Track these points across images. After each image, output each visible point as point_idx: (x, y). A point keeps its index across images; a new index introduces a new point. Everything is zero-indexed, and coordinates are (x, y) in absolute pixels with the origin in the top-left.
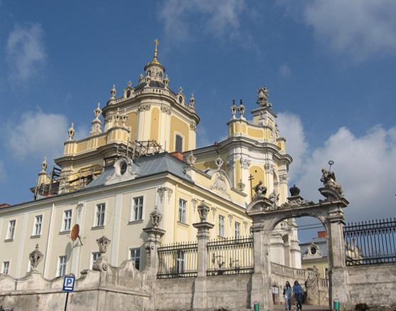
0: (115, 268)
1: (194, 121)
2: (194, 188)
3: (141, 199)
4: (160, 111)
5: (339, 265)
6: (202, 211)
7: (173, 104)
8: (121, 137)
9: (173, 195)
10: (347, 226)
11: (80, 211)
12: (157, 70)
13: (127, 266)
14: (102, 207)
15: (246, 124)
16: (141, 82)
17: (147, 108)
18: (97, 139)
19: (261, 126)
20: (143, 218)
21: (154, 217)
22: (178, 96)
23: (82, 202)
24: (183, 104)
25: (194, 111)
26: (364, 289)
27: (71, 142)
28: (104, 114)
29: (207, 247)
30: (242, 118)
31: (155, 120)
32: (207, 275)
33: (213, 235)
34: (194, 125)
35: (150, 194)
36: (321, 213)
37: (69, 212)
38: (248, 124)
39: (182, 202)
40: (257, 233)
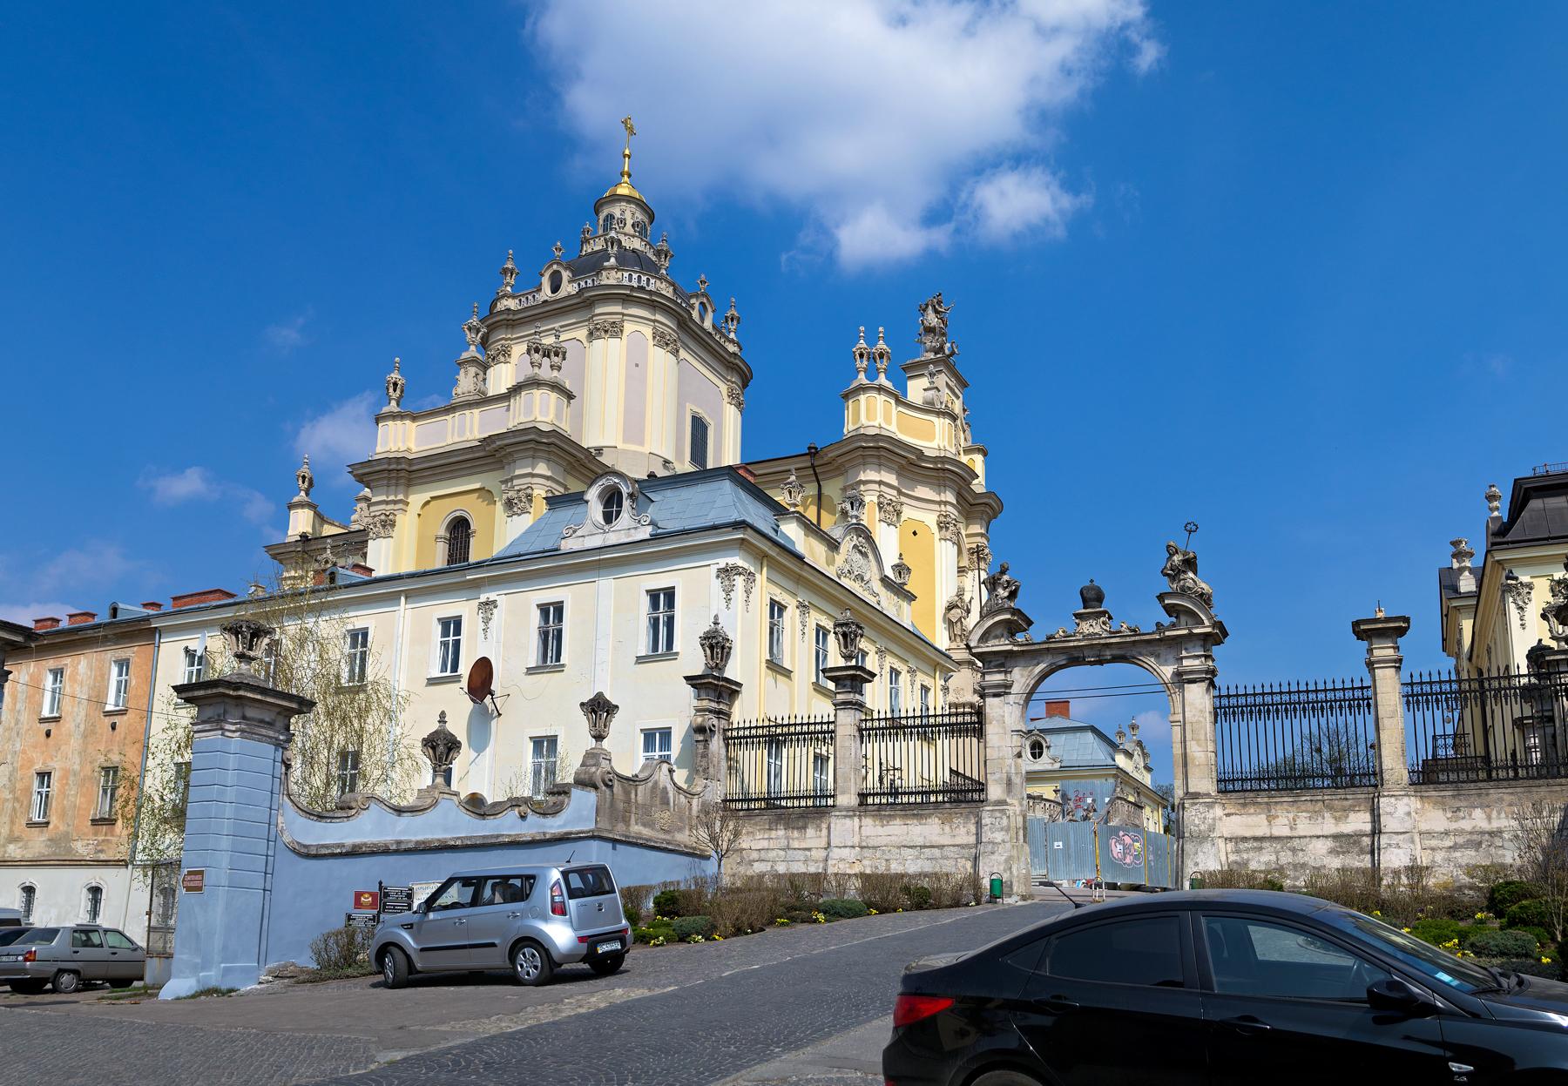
0: (628, 779)
5: (1202, 790)
6: (845, 635)
9: (756, 591)
10: (1224, 692)
11: (487, 621)
13: (656, 777)
14: (552, 613)
16: (587, 249)
17: (614, 330)
18: (476, 411)
21: (712, 647)
23: (492, 596)
26: (1261, 849)
27: (393, 416)
28: (484, 343)
29: (860, 730)
32: (861, 804)
33: (875, 696)
36: (1157, 656)
37: (452, 626)
39: (776, 608)
40: (996, 700)
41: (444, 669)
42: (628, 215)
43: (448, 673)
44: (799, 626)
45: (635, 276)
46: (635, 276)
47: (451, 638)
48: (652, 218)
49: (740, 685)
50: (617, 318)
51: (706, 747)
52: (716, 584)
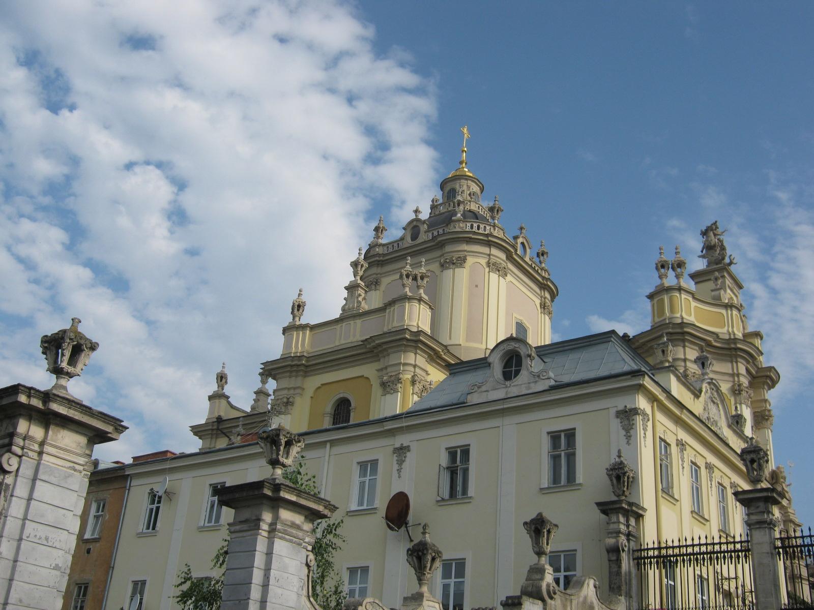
1: (547, 295)
2: (685, 417)
3: (571, 434)
4: (487, 270)
7: (510, 257)
8: (418, 317)
9: (650, 424)
11: (400, 462)
12: (469, 187)
15: (691, 299)
17: (460, 262)
18: (359, 322)
19: (717, 302)
20: (580, 478)
21: (618, 478)
22: (520, 240)
24: (527, 259)
25: (547, 276)
30: (683, 284)
31: (476, 287)
34: (548, 303)
35: (592, 424)
37: (368, 467)
38: (694, 298)
41: (361, 503)
42: (465, 188)
43: (365, 507)
44: (680, 462)
45: (475, 225)
46: (475, 225)
47: (368, 478)
48: (482, 190)
49: (644, 510)
50: (461, 254)
51: (620, 567)
52: (615, 424)
